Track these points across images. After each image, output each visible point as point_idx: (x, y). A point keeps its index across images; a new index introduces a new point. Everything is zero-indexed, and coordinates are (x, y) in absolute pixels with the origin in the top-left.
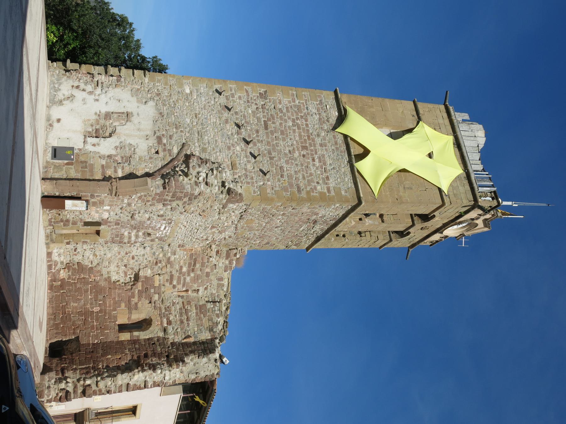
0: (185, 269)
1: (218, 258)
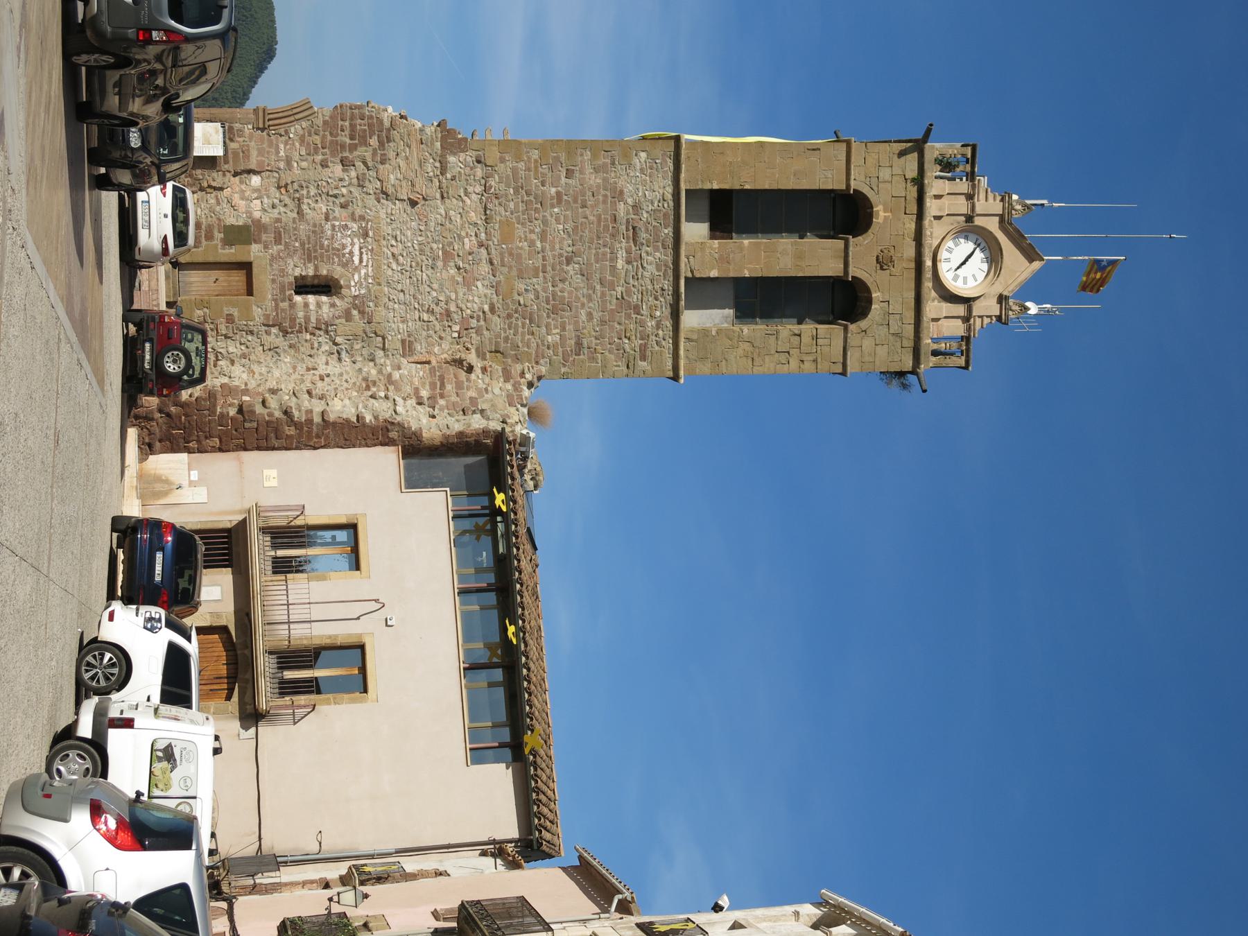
1: (487, 380)
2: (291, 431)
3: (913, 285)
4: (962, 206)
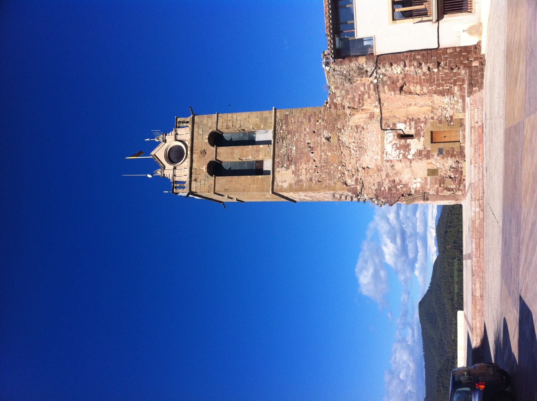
0: (366, 96)
2: (418, 57)
3: (194, 145)
4: (177, 174)
